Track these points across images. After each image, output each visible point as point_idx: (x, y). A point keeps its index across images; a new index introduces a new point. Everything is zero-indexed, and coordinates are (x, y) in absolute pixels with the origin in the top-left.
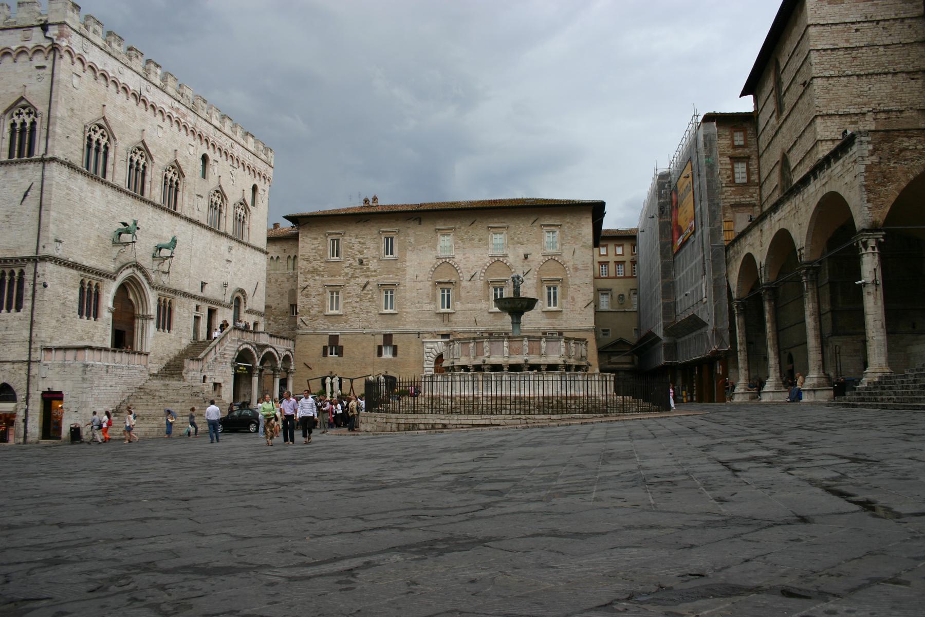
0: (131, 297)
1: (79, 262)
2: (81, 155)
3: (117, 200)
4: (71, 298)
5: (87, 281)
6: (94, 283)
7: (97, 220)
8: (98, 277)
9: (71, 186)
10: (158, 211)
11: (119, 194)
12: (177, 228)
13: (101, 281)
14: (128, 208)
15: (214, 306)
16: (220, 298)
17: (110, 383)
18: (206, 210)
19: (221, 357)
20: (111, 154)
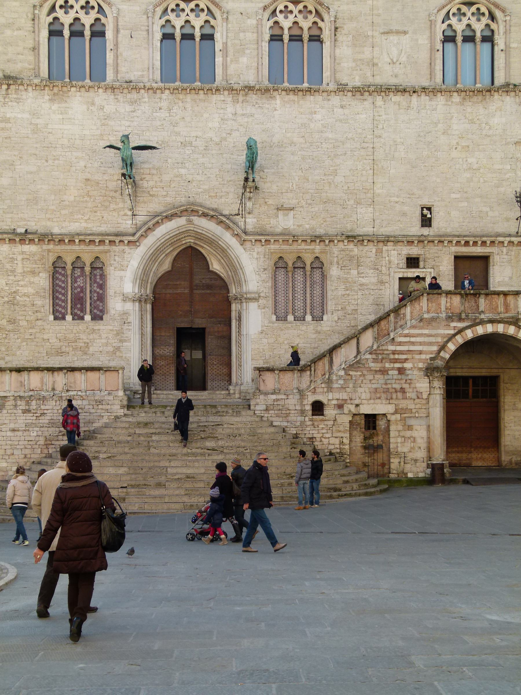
0: (215, 266)
1: (41, 230)
2: (31, 58)
3: (128, 108)
4: (30, 290)
5: (69, 259)
6: (87, 259)
7: (79, 154)
8: (92, 247)
9: (8, 116)
10: (253, 97)
11: (134, 95)
12: (318, 117)
13: (106, 252)
14: (164, 114)
15: (478, 250)
16: (501, 228)
17: (12, 426)
18: (424, 55)
19: (375, 360)
20: (109, 35)
